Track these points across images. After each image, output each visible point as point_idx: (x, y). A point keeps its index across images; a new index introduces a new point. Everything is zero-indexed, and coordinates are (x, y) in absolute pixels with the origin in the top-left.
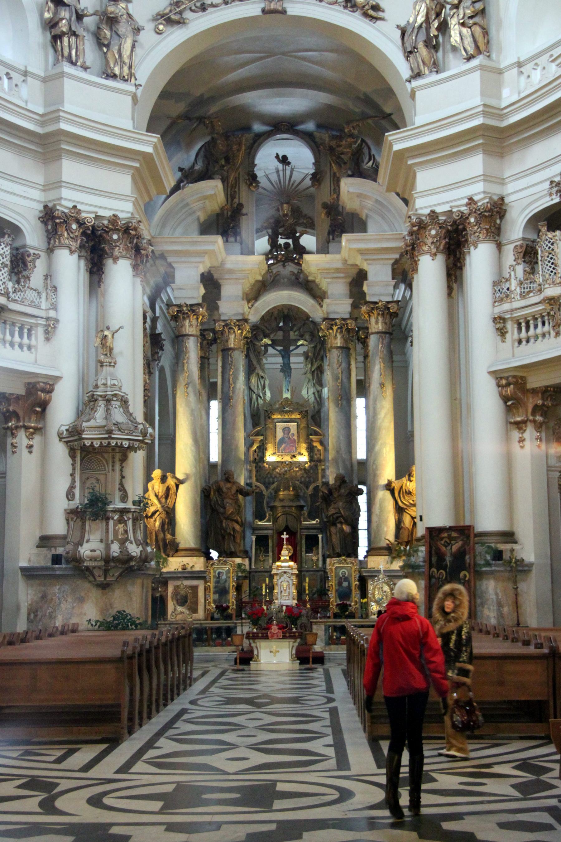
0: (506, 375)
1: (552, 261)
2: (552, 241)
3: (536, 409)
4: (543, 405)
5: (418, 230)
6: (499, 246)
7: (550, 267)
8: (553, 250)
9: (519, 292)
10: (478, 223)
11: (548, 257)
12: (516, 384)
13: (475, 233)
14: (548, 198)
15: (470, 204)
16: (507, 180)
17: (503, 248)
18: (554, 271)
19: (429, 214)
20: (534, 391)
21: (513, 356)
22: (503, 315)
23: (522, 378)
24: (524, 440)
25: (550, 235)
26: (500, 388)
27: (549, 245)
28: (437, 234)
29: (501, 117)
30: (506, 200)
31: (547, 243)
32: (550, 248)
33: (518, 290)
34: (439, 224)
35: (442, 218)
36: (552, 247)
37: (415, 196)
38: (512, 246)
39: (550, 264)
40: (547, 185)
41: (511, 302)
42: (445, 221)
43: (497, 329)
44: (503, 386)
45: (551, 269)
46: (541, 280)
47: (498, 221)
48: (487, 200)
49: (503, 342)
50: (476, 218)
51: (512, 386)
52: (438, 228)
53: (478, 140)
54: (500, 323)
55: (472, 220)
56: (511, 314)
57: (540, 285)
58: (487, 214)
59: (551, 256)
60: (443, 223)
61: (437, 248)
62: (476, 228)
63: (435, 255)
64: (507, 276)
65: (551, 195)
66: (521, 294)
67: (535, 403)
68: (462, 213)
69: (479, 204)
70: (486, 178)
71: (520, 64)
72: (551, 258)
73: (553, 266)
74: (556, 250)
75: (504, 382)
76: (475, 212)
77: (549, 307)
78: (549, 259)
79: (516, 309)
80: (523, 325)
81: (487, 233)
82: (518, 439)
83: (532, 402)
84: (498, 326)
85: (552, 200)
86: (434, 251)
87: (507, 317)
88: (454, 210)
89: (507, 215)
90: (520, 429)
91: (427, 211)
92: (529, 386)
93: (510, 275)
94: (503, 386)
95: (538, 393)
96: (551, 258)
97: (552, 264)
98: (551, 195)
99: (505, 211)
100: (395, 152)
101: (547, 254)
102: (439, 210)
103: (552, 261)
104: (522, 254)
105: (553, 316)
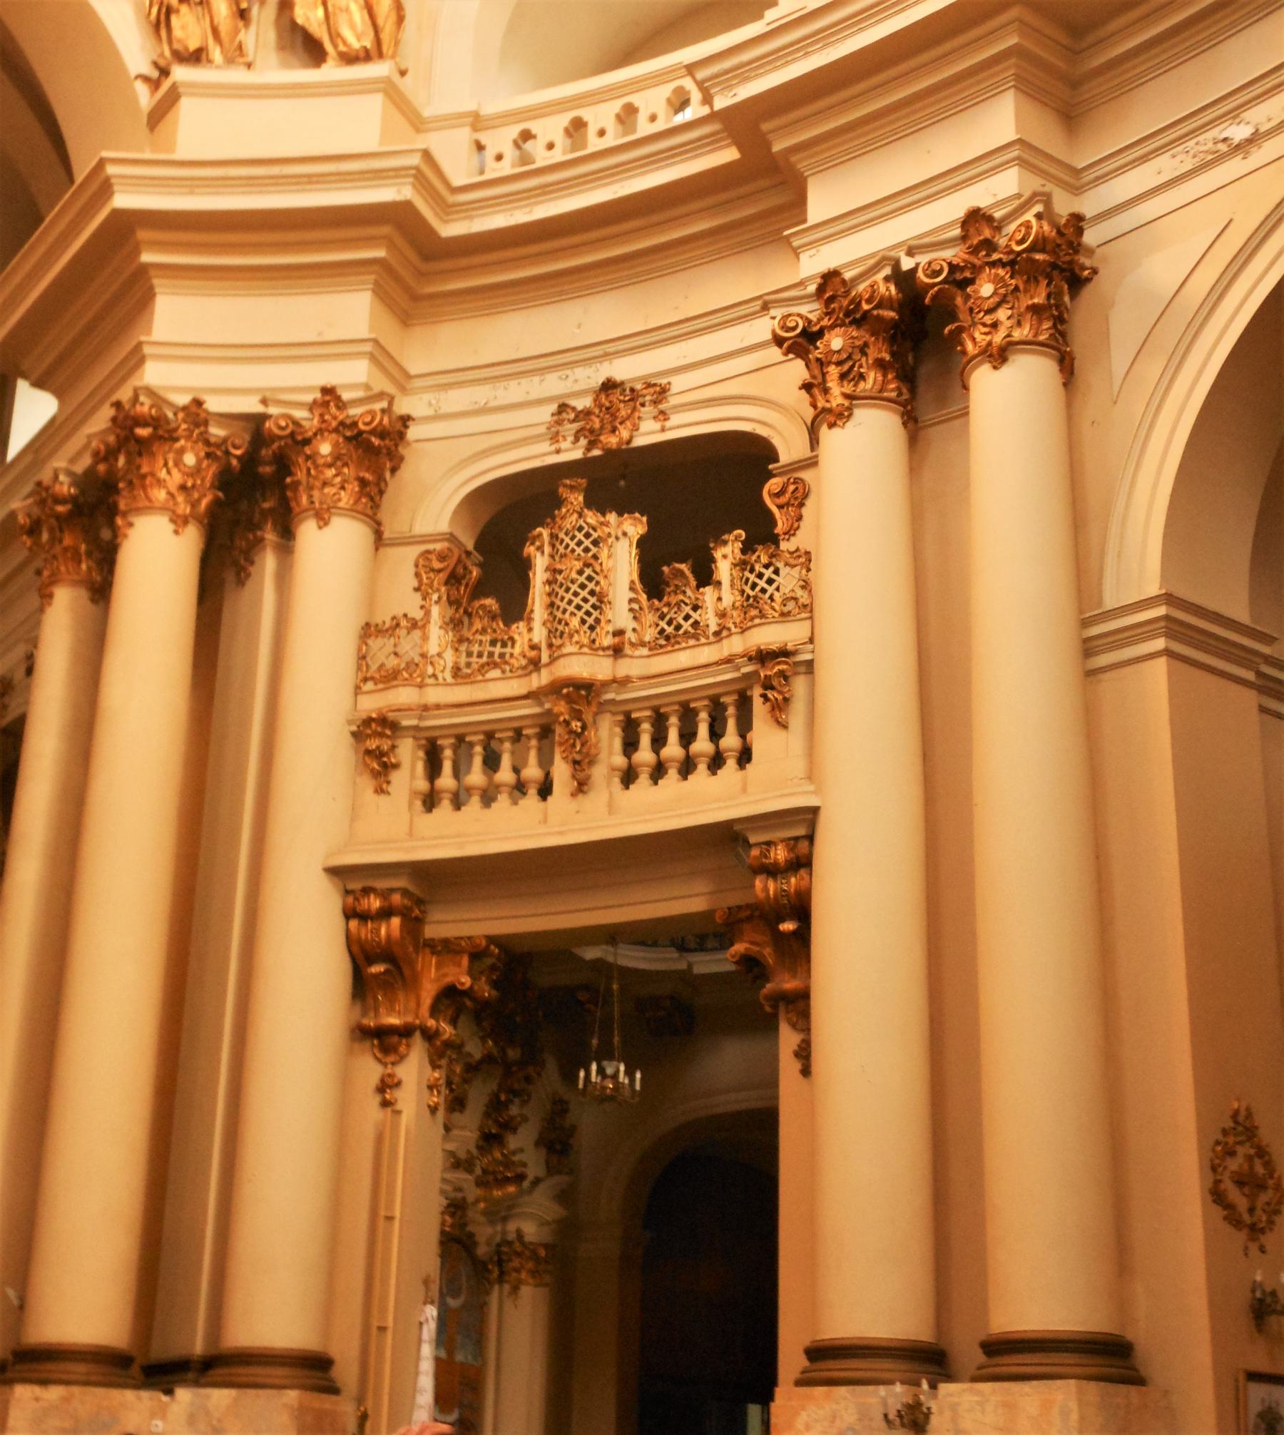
0: (381, 884)
1: (591, 586)
2: (595, 535)
3: (450, 996)
4: (468, 993)
5: (156, 437)
6: (379, 540)
7: (585, 600)
8: (595, 557)
9: (450, 665)
10: (337, 459)
11: (580, 572)
12: (404, 913)
13: (325, 484)
14: (545, 447)
15: (326, 404)
16: (417, 383)
17: (382, 550)
18: (595, 614)
19: (184, 408)
20: (446, 948)
21: (410, 834)
22: (391, 716)
23: (419, 902)
24: (398, 1084)
25: (592, 518)
26: (354, 924)
27: (587, 543)
28: (197, 470)
29: (448, 211)
30: (413, 433)
31: (580, 536)
32: (587, 550)
33: (449, 656)
34: (207, 443)
35: (217, 432)
36: (594, 550)
37: (147, 350)
38: (413, 552)
39: (584, 593)
40: (545, 414)
41: (421, 686)
42: (225, 440)
43: (368, 752)
44: (364, 917)
45: (587, 607)
46: (539, 634)
47: (388, 475)
48: (384, 404)
49: (380, 791)
50: (335, 445)
51: (396, 921)
52: (202, 454)
53: (377, 246)
54: (382, 735)
55: (325, 448)
56: (421, 718)
57: (534, 647)
58: (376, 441)
59: (588, 571)
60: (218, 446)
61: (194, 505)
62: (333, 471)
63: (186, 522)
64: (418, 614)
65: (555, 438)
66: (456, 671)
67: (449, 979)
68: (296, 423)
69: (354, 412)
70: (380, 356)
71: (477, 121)
72: (590, 579)
73: (593, 600)
74: (603, 555)
75: (375, 903)
76: (336, 430)
77: (561, 708)
78: (582, 579)
79: (438, 707)
80: (448, 753)
81: (362, 493)
82: (374, 1080)
83: (432, 977)
84: (372, 744)
85: (558, 451)
86: (183, 508)
87: (405, 723)
88: (273, 410)
89: (406, 472)
90: (387, 1049)
91: (182, 400)
92: (431, 931)
93: (428, 613)
94: (364, 917)
95: (459, 952)
96: (590, 579)
97: (592, 593)
98: (555, 438)
99: (402, 459)
100: (117, 213)
101: (578, 565)
102: (214, 405)
103: (591, 586)
104: (443, 576)
105: (579, 735)
